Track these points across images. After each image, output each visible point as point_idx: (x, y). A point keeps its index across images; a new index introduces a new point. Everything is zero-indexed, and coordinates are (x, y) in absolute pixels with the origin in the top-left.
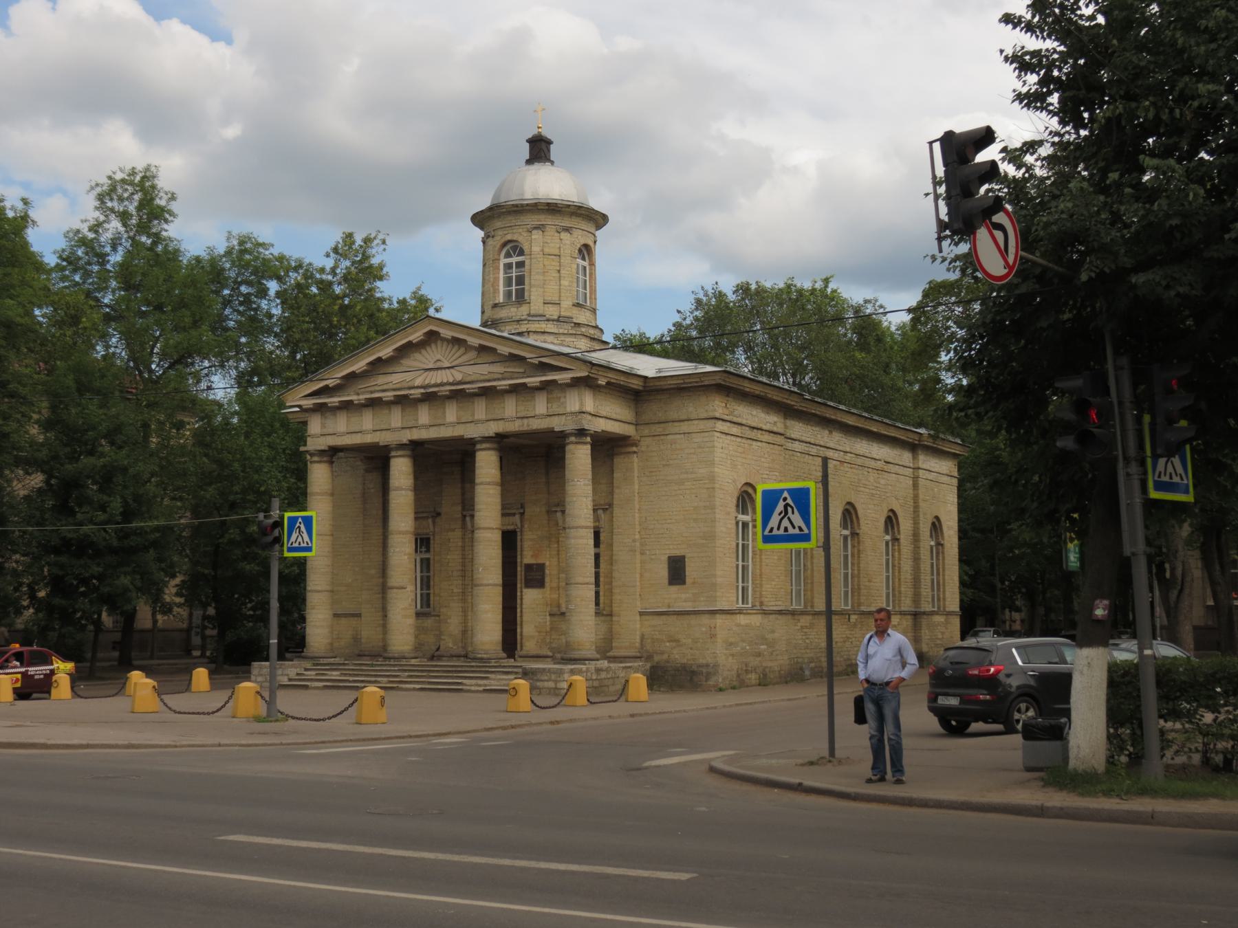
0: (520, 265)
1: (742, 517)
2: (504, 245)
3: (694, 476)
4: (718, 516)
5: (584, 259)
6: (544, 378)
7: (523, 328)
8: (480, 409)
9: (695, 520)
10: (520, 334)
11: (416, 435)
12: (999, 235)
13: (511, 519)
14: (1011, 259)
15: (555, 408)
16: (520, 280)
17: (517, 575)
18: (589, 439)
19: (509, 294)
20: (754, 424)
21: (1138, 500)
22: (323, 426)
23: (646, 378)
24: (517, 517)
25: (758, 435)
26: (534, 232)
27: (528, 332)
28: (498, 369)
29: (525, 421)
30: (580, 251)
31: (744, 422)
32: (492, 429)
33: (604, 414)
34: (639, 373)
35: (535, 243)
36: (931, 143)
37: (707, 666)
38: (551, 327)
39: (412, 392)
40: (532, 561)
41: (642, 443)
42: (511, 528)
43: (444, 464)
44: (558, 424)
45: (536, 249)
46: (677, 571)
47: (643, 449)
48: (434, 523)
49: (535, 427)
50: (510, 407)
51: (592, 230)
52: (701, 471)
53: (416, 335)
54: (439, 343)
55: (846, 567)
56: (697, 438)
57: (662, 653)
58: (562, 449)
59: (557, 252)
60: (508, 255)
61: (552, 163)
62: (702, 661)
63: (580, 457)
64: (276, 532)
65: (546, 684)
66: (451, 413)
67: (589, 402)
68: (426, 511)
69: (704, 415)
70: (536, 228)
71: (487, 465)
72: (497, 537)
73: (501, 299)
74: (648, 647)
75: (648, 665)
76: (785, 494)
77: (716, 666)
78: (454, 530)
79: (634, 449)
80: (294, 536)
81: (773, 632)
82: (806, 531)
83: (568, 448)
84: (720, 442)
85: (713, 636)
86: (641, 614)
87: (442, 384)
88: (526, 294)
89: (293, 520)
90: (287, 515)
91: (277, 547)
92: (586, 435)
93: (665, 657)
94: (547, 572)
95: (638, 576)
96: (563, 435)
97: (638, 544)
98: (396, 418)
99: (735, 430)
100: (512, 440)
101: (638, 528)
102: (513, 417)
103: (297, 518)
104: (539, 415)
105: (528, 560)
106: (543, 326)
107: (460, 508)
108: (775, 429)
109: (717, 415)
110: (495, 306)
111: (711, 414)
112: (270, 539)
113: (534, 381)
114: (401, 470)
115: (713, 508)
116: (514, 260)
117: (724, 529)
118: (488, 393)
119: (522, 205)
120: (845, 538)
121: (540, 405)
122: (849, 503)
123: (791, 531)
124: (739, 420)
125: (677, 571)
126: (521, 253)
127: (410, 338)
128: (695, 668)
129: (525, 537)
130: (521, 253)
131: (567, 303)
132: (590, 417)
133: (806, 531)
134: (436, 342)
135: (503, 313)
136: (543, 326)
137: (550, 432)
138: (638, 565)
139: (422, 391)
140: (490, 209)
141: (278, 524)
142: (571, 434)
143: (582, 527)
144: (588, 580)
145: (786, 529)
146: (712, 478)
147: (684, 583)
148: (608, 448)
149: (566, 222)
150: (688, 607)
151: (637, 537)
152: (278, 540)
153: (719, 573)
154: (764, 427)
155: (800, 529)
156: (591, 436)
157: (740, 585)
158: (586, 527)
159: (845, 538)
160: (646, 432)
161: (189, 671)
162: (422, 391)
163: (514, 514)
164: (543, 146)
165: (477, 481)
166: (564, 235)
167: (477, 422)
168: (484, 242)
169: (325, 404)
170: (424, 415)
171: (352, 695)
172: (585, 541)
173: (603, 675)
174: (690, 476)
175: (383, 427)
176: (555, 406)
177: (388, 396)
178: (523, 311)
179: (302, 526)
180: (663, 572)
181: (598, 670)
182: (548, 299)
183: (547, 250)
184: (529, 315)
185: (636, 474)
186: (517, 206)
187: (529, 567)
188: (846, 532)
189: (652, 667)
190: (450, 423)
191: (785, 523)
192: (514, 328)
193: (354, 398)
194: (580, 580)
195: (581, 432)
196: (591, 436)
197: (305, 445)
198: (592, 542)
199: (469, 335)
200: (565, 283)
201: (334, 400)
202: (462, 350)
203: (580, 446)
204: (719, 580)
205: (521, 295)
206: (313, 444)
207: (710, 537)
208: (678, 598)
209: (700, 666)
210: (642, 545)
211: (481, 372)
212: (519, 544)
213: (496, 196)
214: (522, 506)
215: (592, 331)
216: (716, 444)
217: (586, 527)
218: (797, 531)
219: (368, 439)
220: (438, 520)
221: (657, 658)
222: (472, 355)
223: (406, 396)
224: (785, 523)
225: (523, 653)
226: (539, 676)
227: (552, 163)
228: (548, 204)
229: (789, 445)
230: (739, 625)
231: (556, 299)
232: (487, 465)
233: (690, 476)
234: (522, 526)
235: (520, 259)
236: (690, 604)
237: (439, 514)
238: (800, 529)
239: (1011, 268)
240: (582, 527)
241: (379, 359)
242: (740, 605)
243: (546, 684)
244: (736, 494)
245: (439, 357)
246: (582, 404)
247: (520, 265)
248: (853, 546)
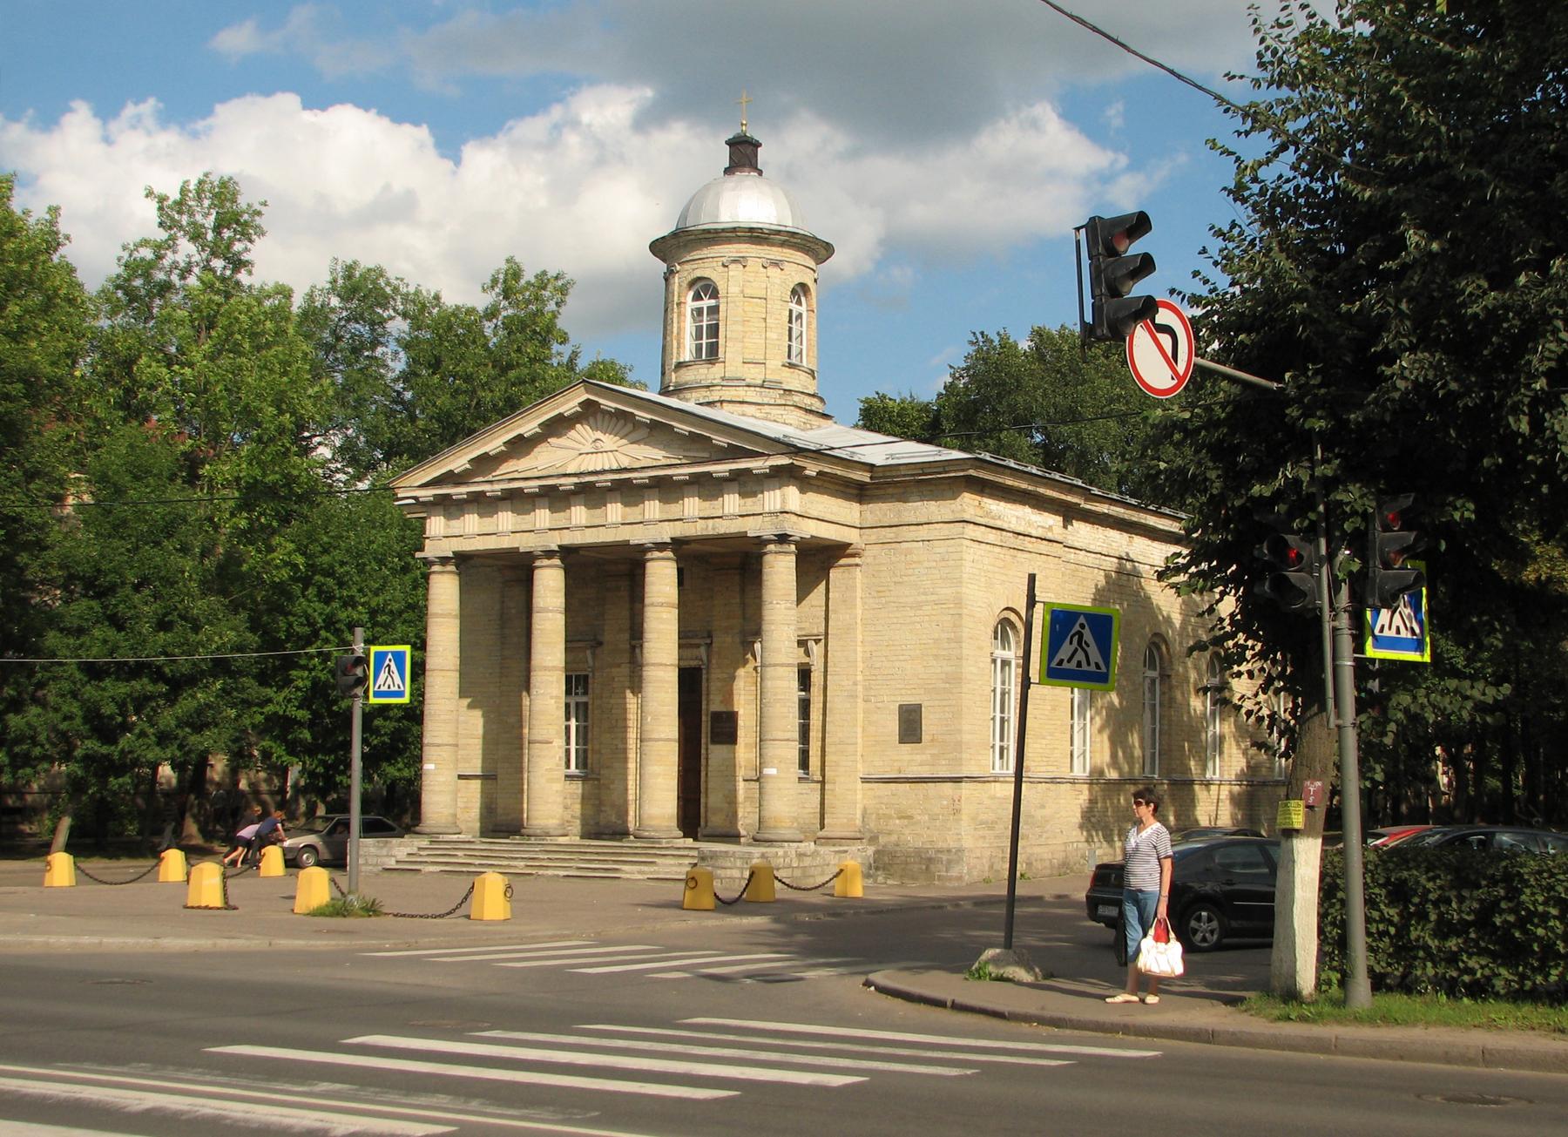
1: (1001, 653)
2: (692, 284)
3: (934, 597)
4: (965, 652)
5: (799, 303)
6: (734, 466)
7: (715, 395)
8: (653, 508)
9: (936, 657)
10: (709, 404)
11: (569, 539)
12: (1165, 340)
13: (695, 652)
14: (1181, 368)
16: (714, 330)
17: (705, 726)
18: (793, 547)
19: (699, 348)
20: (1020, 529)
21: (1347, 663)
22: (447, 526)
23: (873, 466)
24: (703, 650)
25: (1027, 543)
26: (732, 266)
27: (722, 402)
30: (794, 292)
31: (1005, 526)
32: (666, 533)
33: (815, 514)
34: (863, 460)
35: (731, 283)
36: (1078, 229)
37: (949, 851)
38: (751, 395)
41: (866, 553)
42: (694, 663)
43: (606, 579)
44: (753, 527)
45: (734, 290)
46: (910, 725)
48: (594, 654)
50: (692, 506)
51: (812, 264)
52: (944, 591)
53: (569, 404)
54: (599, 416)
55: (1154, 723)
56: (940, 548)
57: (890, 833)
58: (760, 557)
59: (762, 294)
60: (697, 297)
61: (760, 173)
62: (940, 845)
63: (780, 570)
64: (359, 672)
65: (729, 873)
66: (615, 511)
67: (791, 497)
68: (579, 638)
70: (734, 261)
71: (662, 580)
72: (672, 676)
73: (687, 356)
74: (872, 825)
75: (871, 850)
76: (1082, 620)
77: (960, 850)
78: (619, 666)
79: (857, 560)
80: (383, 676)
81: (1043, 807)
82: (1104, 669)
83: (767, 558)
84: (972, 553)
85: (957, 812)
86: (865, 780)
87: (603, 472)
88: (721, 350)
89: (381, 657)
90: (374, 649)
91: (359, 691)
92: (789, 543)
93: (894, 838)
94: (740, 723)
95: (859, 730)
96: (760, 542)
97: (860, 688)
98: (542, 517)
99: (992, 536)
100: (693, 546)
101: (860, 666)
102: (696, 516)
103: (386, 653)
104: (731, 515)
105: (716, 706)
106: (741, 393)
107: (627, 636)
108: (1050, 536)
109: (967, 517)
110: (680, 365)
111: (959, 517)
112: (351, 679)
113: (721, 469)
114: (550, 585)
115: (959, 641)
116: (707, 303)
117: (974, 670)
119: (716, 231)
120: (1153, 681)
121: (732, 502)
122: (1156, 634)
123: (1085, 667)
124: (999, 524)
125: (910, 725)
127: (561, 410)
128: (931, 854)
129: (713, 676)
130: (715, 294)
131: (776, 360)
132: (794, 518)
133: (1104, 669)
134: (594, 415)
135: (688, 376)
136: (741, 393)
137: (742, 537)
138: (860, 716)
139: (576, 480)
140: (674, 235)
141: (362, 661)
142: (770, 542)
143: (782, 665)
144: (788, 735)
145: (1079, 664)
146: (958, 602)
147: (919, 741)
148: (818, 560)
149: (775, 253)
150: (925, 772)
151: (860, 678)
152: (362, 681)
153: (966, 728)
154: (1034, 533)
155: (1097, 666)
156: (796, 543)
157: (998, 744)
158: (789, 665)
159: (1153, 681)
160: (873, 539)
161: (155, 853)
162: (576, 480)
163: (698, 646)
164: (749, 150)
165: (647, 601)
166: (773, 271)
167: (649, 523)
168: (666, 280)
169: (449, 496)
171: (469, 880)
172: (785, 684)
173: (807, 862)
174: (931, 598)
177: (531, 486)
178: (713, 373)
179: (393, 664)
180: (893, 725)
181: (801, 855)
182: (749, 357)
183: (748, 292)
184: (723, 379)
185: (859, 593)
186: (708, 231)
188: (1155, 674)
189: (877, 852)
190: (613, 524)
191: (1080, 656)
192: (703, 395)
194: (780, 735)
195: (783, 539)
196: (796, 543)
197: (422, 549)
198: (795, 684)
200: (772, 335)
201: (460, 491)
202: (630, 426)
203: (781, 557)
204: (966, 737)
205: (713, 350)
206: (431, 550)
207: (955, 680)
208: (912, 760)
209: (939, 851)
210: (866, 689)
211: (646, 457)
212: (704, 684)
213: (684, 216)
214: (710, 636)
215: (808, 400)
216: (965, 556)
217: (789, 665)
218: (1093, 668)
219: (505, 543)
220: (598, 651)
221: (882, 840)
223: (554, 488)
224: (1080, 656)
225: (708, 831)
226: (720, 862)
227: (760, 173)
228: (751, 230)
229: (1071, 555)
230: (993, 798)
231: (760, 358)
232: (662, 580)
233: (931, 598)
234: (709, 661)
235: (713, 302)
236: (927, 768)
237: (601, 644)
238: (1097, 666)
239: (1180, 379)
240: (782, 665)
241: (520, 436)
242: (997, 770)
243: (729, 873)
244: (993, 622)
246: (784, 501)
247: (714, 310)
248: (1163, 693)
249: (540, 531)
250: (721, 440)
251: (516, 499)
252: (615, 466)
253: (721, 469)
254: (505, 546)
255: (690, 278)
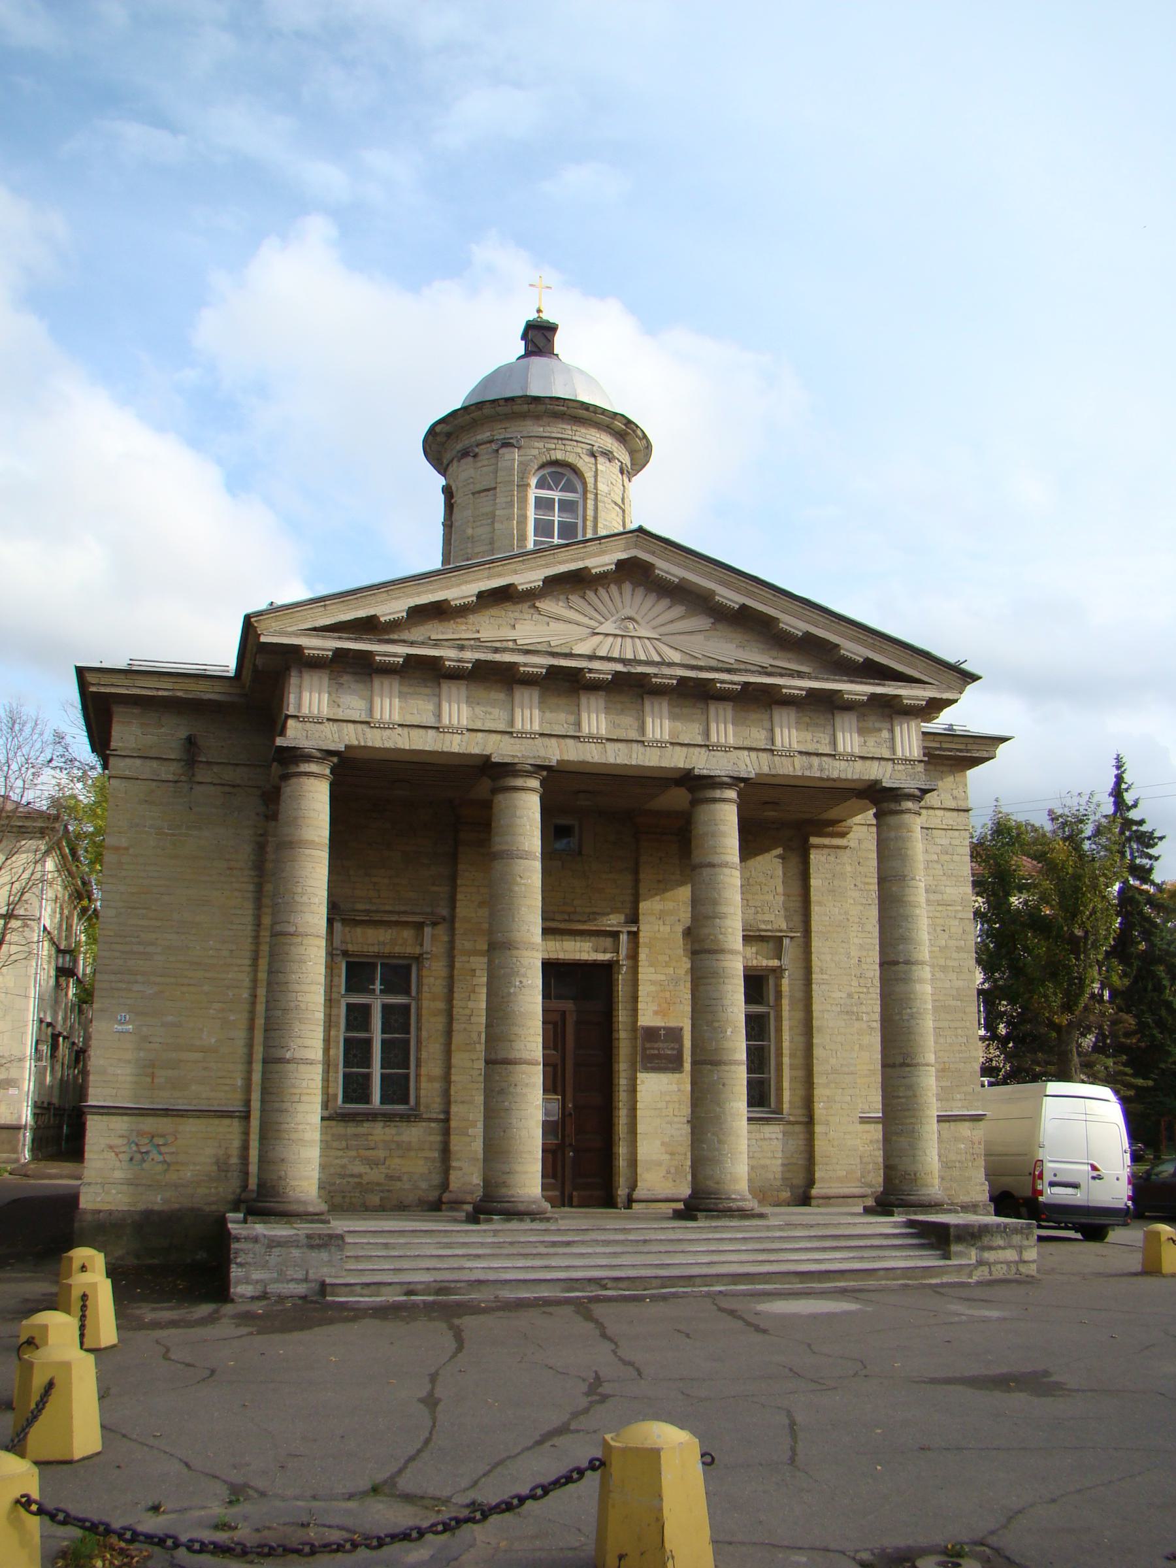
0: (566, 506)
6: (879, 690)
11: (573, 753)
15: (872, 750)
22: (334, 703)
28: (757, 656)
29: (815, 761)
39: (596, 665)
40: (657, 1022)
47: (852, 844)
49: (835, 775)
52: (948, 890)
66: (660, 724)
69: (953, 805)
98: (530, 715)
102: (791, 748)
118: (758, 700)
126: (569, 488)
127: (588, 563)
162: (620, 667)
167: (730, 748)
169: (370, 654)
170: (596, 719)
175: (489, 725)
176: (871, 741)
187: (651, 1033)
190: (660, 741)
193: (448, 654)
197: (282, 733)
199: (723, 583)
206: (294, 735)
219: (455, 744)
222: (701, 622)
226: (986, 1241)
245: (628, 612)
249: (522, 735)
250: (855, 650)
251: (496, 677)
252: (657, 658)
253: (859, 690)
254: (455, 749)
255: (544, 459)
